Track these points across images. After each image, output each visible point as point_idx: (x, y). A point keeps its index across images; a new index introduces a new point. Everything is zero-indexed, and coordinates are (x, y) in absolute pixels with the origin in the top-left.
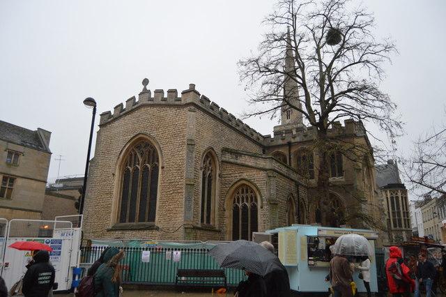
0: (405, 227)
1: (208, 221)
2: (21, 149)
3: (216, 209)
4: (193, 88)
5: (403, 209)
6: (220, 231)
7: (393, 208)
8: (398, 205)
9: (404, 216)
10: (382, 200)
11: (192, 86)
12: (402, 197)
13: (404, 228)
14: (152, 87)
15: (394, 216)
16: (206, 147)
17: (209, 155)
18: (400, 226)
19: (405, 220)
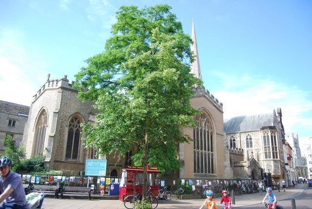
0: (274, 157)
1: (75, 157)
2: (16, 117)
3: (81, 150)
4: (65, 80)
5: (272, 144)
6: (81, 164)
7: (265, 145)
8: (268, 142)
9: (273, 150)
10: (258, 139)
11: (66, 76)
12: (272, 137)
13: (272, 159)
14: (51, 79)
15: (266, 150)
16: (72, 112)
17: (75, 119)
18: (270, 157)
19: (273, 153)
